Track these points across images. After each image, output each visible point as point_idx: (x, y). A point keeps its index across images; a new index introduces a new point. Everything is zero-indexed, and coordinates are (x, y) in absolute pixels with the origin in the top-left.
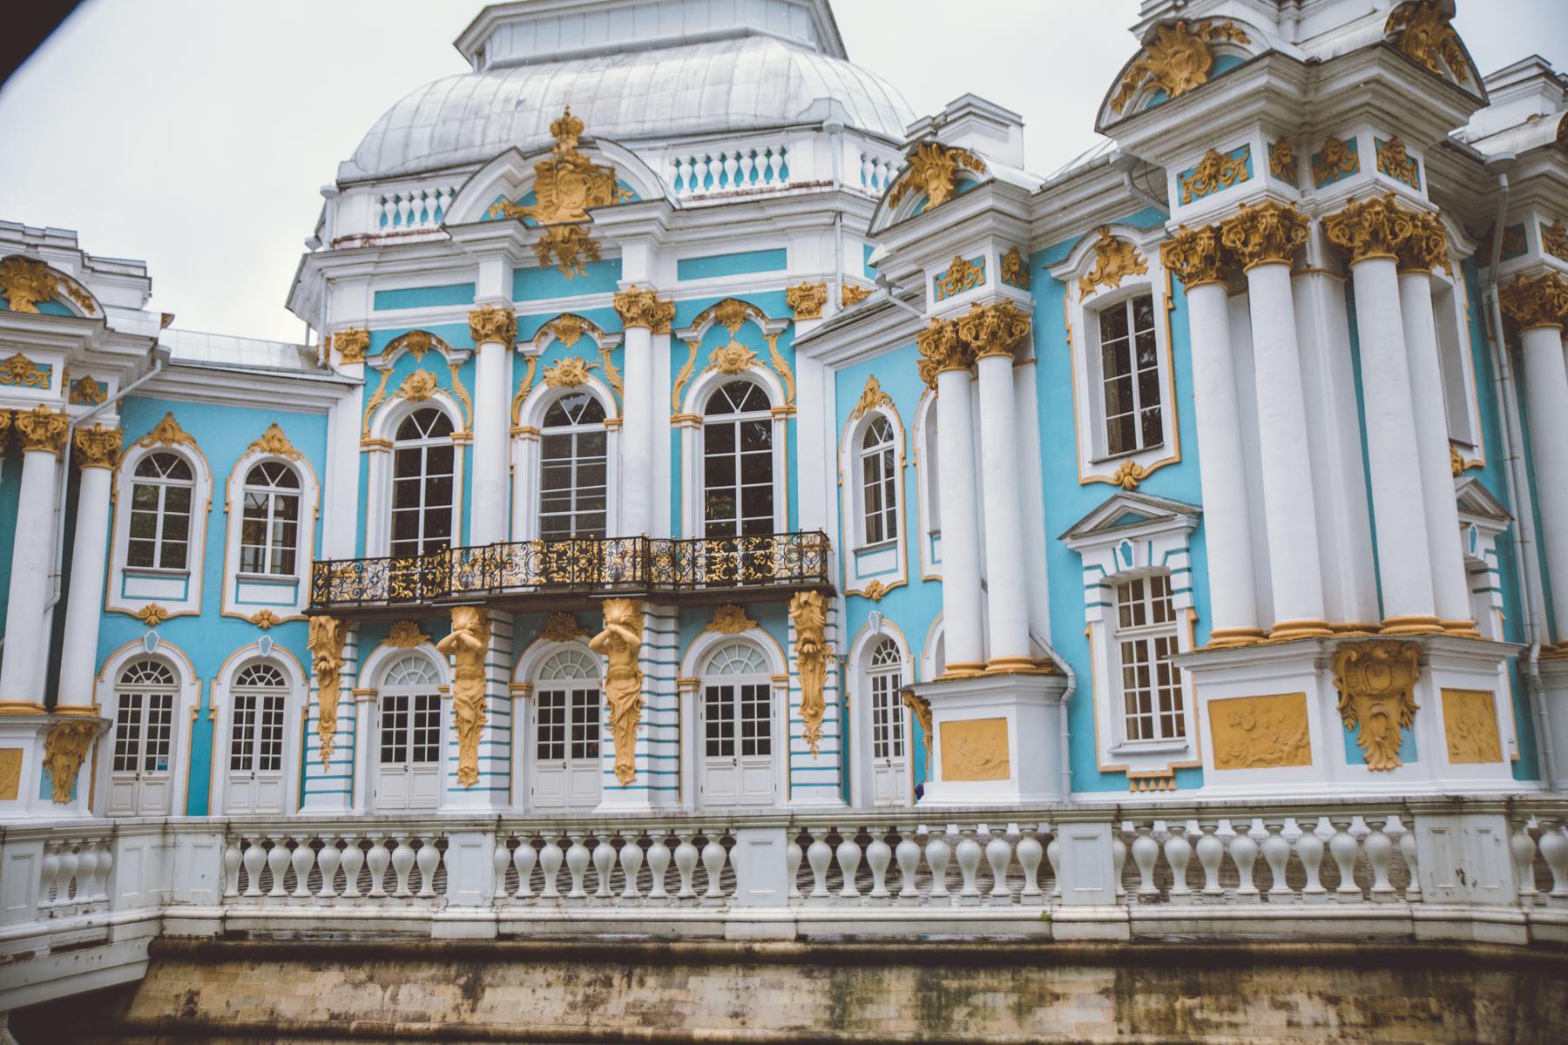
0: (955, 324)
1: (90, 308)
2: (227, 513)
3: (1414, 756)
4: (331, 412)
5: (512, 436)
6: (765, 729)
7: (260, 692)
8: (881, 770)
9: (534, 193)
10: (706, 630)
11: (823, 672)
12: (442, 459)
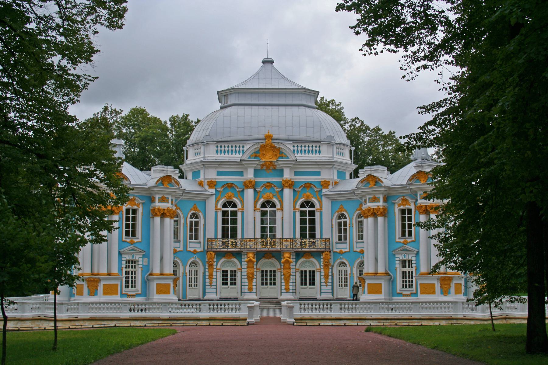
0: (374, 209)
1: (178, 185)
2: (187, 226)
3: (450, 294)
4: (207, 201)
5: (254, 210)
6: (314, 280)
7: (193, 268)
8: (340, 290)
9: (259, 150)
10: (301, 258)
11: (329, 269)
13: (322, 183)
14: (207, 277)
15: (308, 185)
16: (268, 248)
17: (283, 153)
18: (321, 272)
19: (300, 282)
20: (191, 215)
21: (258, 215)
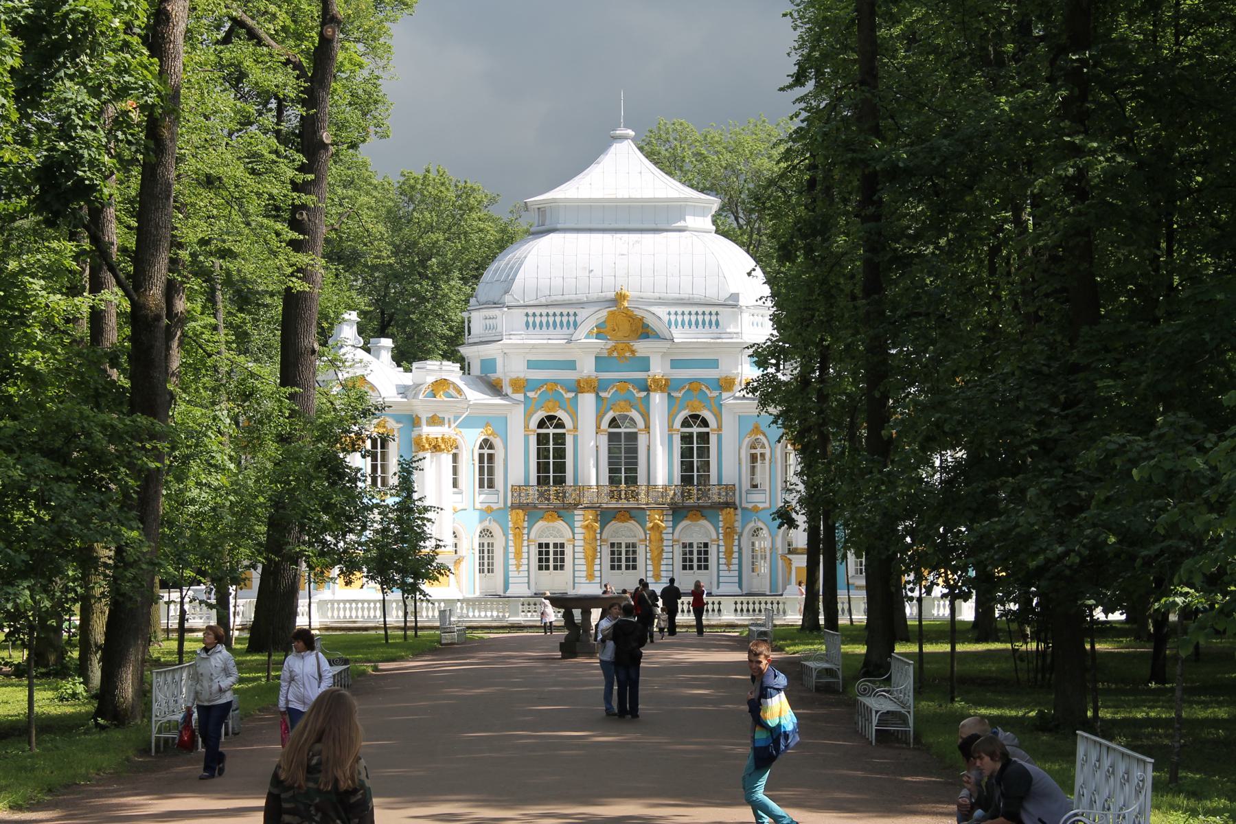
6: (706, 560)
11: (734, 539)
14: (511, 556)
16: (624, 504)
18: (718, 546)
19: (681, 564)
20: (481, 445)
21: (604, 441)
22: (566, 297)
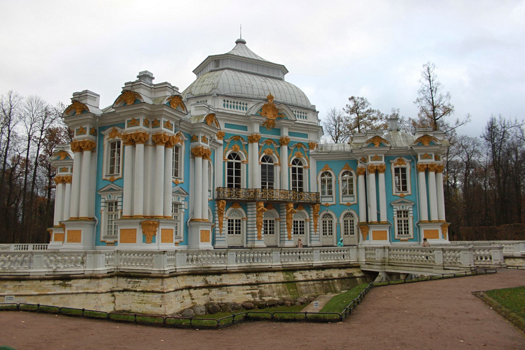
0: (377, 166)
1: (218, 127)
4: (216, 151)
12: (238, 165)
13: (310, 144)
15: (300, 145)
17: (280, 114)
18: (310, 222)
22: (243, 95)
